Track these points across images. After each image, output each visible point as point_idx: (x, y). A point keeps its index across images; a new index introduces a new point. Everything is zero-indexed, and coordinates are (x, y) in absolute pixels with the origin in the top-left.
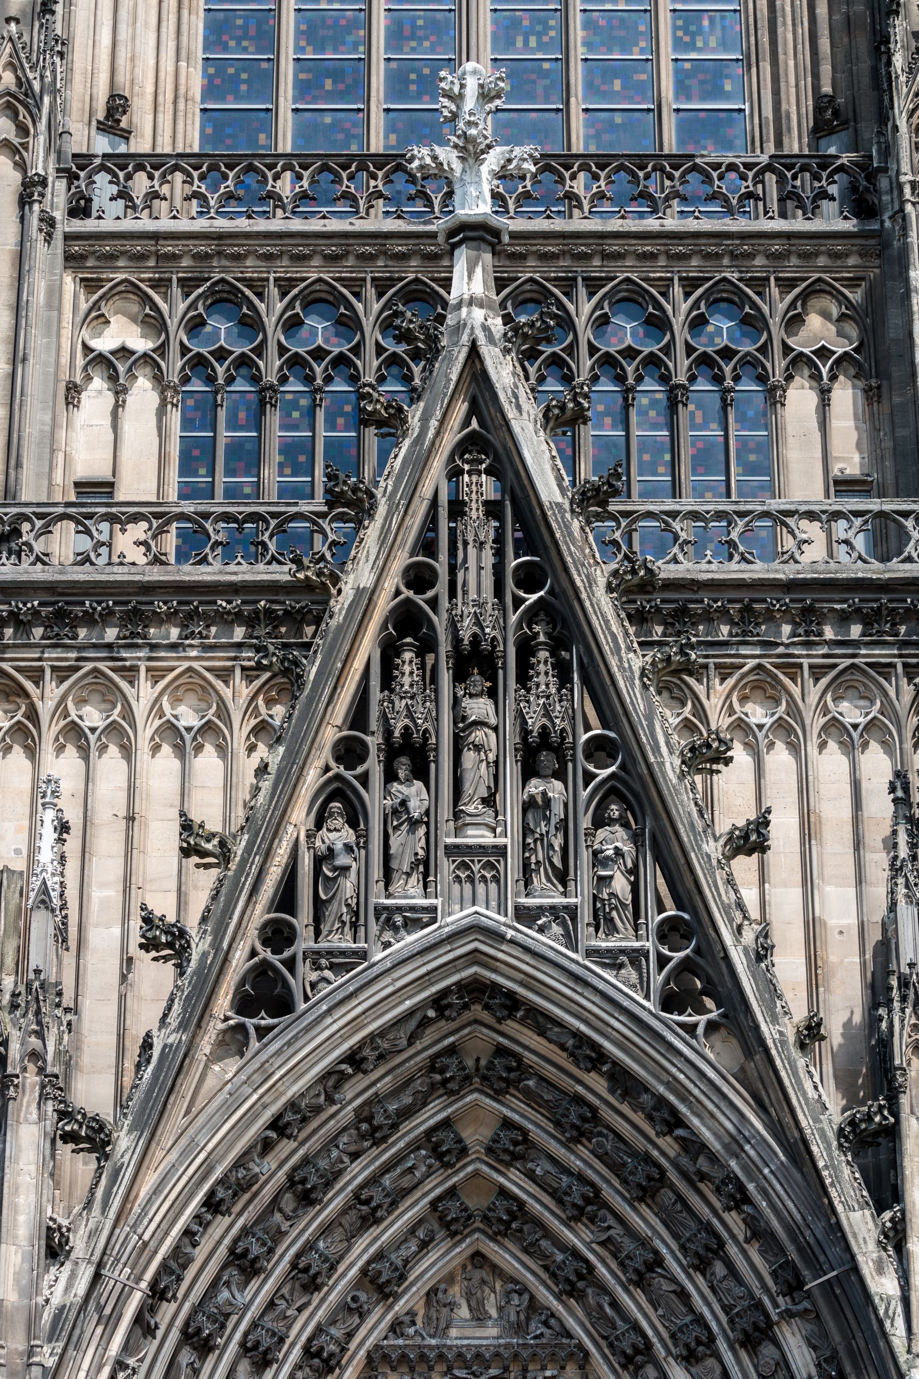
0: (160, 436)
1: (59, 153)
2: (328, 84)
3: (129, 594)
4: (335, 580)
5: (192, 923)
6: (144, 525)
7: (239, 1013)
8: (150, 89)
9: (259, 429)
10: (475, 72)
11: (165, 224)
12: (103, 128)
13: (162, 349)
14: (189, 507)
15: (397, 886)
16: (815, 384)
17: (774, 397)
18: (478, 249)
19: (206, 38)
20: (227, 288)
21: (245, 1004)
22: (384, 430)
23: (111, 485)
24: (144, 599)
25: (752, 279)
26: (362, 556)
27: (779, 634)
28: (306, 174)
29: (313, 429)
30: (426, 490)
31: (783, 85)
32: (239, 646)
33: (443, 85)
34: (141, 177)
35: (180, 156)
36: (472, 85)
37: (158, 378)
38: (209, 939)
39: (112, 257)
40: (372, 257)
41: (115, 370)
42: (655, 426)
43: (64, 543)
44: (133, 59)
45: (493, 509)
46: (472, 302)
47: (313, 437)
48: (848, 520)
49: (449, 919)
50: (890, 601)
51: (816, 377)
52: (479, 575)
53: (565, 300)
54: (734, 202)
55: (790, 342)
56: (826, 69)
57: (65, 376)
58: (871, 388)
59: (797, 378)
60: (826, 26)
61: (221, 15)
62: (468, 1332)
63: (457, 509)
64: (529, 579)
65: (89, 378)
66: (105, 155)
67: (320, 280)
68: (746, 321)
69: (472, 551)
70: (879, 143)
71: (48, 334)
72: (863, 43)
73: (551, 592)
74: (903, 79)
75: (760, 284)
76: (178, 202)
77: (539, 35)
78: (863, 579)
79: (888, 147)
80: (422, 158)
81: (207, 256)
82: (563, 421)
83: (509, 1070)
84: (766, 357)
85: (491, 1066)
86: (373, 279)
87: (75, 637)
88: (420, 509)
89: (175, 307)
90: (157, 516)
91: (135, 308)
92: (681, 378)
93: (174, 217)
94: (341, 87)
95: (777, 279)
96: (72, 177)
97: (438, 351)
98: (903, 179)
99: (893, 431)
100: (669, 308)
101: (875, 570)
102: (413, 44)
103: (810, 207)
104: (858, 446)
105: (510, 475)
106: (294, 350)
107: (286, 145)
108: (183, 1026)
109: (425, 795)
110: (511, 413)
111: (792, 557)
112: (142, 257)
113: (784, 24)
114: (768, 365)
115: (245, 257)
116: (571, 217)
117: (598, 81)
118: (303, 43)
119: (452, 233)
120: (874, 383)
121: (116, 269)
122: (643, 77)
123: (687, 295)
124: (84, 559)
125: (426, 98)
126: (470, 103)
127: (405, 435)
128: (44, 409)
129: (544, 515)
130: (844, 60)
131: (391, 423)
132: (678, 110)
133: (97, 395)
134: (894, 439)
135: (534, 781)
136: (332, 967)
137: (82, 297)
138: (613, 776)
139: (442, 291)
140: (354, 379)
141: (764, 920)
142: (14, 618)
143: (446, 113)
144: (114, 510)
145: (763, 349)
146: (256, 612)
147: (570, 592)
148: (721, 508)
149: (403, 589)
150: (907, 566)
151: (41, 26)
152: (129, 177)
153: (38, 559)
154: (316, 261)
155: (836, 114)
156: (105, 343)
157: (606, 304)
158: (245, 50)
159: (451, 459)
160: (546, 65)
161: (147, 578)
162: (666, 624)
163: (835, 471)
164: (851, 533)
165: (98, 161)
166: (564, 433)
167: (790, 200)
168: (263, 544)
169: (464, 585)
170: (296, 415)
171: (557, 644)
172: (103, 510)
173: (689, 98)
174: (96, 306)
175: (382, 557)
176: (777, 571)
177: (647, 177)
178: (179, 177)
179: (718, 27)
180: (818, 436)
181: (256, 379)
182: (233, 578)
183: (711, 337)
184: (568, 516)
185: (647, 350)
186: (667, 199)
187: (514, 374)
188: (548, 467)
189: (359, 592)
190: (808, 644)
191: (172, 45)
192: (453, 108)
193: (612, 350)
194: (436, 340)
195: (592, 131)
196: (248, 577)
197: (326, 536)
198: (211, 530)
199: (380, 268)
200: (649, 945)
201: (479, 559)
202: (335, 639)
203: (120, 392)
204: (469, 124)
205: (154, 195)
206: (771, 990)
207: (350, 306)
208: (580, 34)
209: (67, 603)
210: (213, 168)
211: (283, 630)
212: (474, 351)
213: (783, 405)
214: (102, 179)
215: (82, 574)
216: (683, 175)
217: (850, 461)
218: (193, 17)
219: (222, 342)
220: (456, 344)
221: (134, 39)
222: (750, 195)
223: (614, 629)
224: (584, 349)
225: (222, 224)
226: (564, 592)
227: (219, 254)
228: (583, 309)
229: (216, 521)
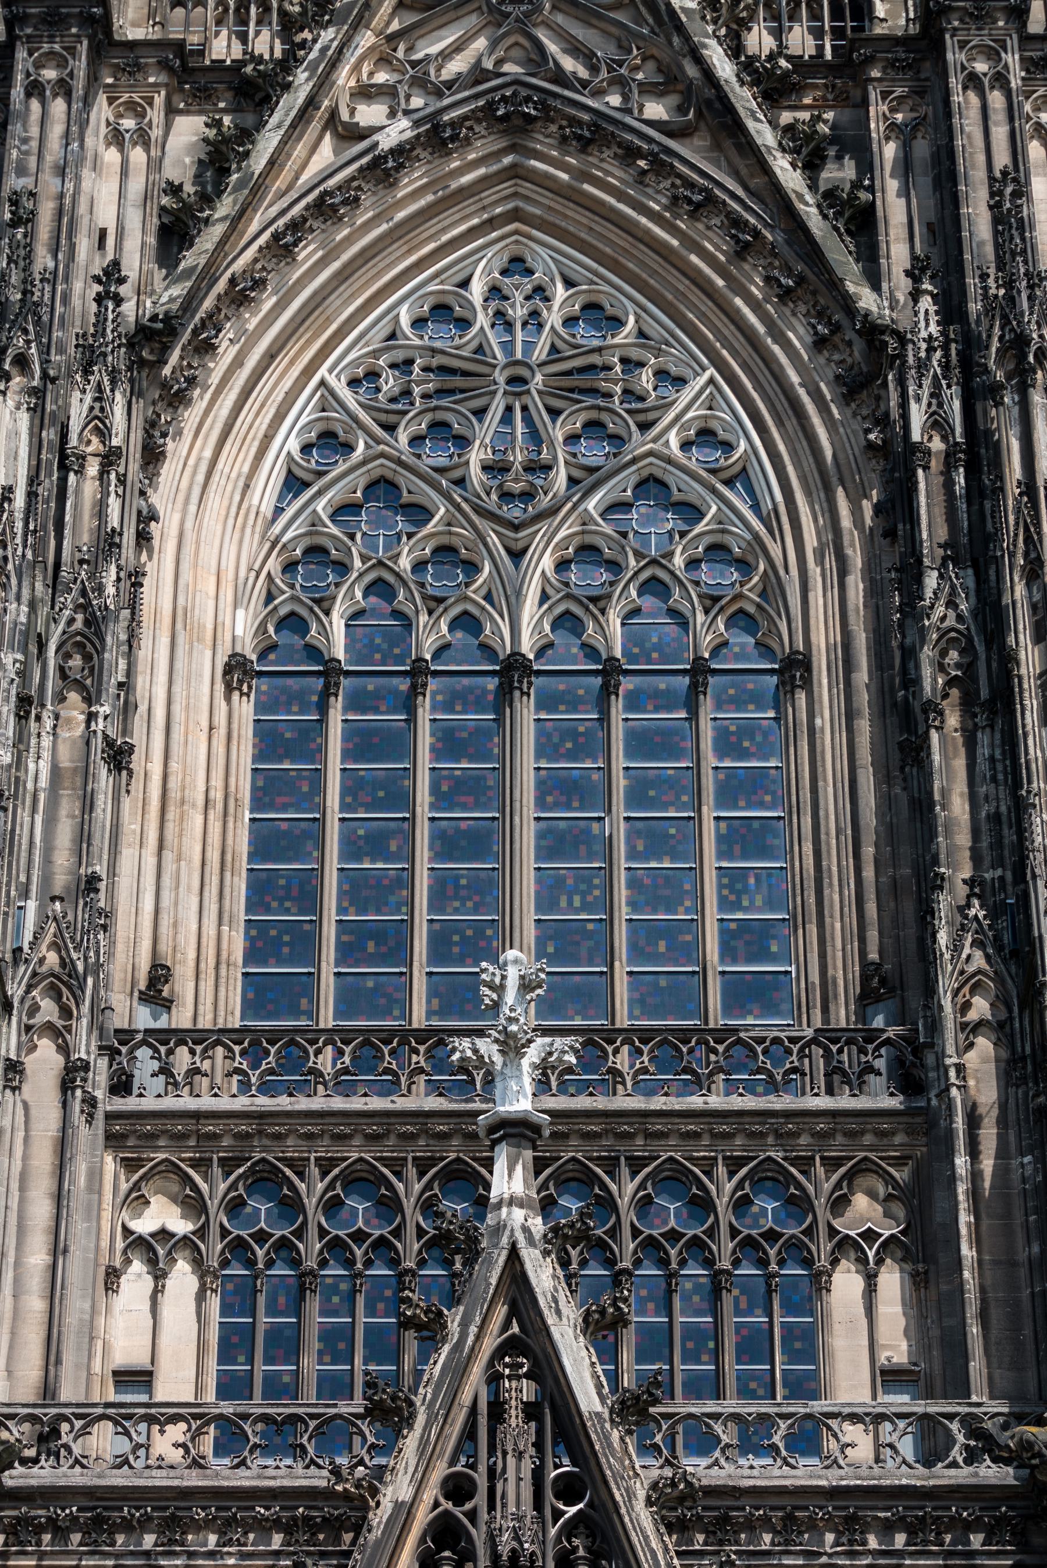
0: (199, 1322)
1: (101, 1029)
2: (371, 946)
3: (167, 1499)
4: (374, 1492)
6: (183, 1426)
8: (192, 955)
9: (298, 1316)
10: (516, 961)
11: (206, 1103)
12: (145, 998)
13: (202, 1232)
14: (227, 1408)
16: (861, 1267)
17: (819, 1282)
18: (518, 1146)
19: (248, 899)
20: (267, 1168)
22: (425, 1333)
23: (150, 1374)
24: (183, 1504)
25: (797, 1158)
26: (401, 1467)
27: (822, 1543)
28: (347, 1050)
29: (353, 1315)
30: (466, 1397)
31: (829, 949)
32: (277, 1554)
33: (484, 976)
34: (183, 1052)
35: (221, 1031)
36: (513, 974)
37: (198, 1262)
39: (152, 1136)
40: (413, 1137)
41: (155, 1253)
42: (698, 1313)
43: (104, 1441)
44: (175, 925)
45: (531, 1411)
46: (512, 1201)
47: (353, 1323)
48: (893, 1422)
50: (934, 1509)
51: (862, 1260)
52: (518, 1486)
53: (607, 1179)
54: (779, 1078)
55: (837, 1224)
56: (873, 935)
57: (105, 1261)
58: (918, 1274)
59: (843, 1262)
60: (873, 890)
61: (264, 874)
63: (497, 1411)
64: (568, 1489)
65: (128, 1262)
66: (146, 1031)
67: (361, 1160)
68: (791, 1200)
69: (511, 1461)
70: (925, 1017)
71: (88, 1219)
72: (909, 908)
73: (590, 1505)
74: (947, 956)
75: (805, 1164)
76: (218, 1080)
77: (584, 895)
78: (907, 1486)
79: (934, 1021)
80: (463, 1051)
81: (248, 1136)
82: (602, 1328)
84: (811, 1240)
86: (414, 1159)
87: (113, 1544)
88: (460, 1417)
89: (216, 1188)
90: (196, 1417)
91: (175, 1188)
92: (725, 1264)
93: (216, 1095)
94: (384, 949)
95: (822, 1158)
96: (112, 1053)
97: (478, 1253)
98: (948, 1061)
99: (940, 1319)
100: (712, 1188)
101: (917, 1477)
102: (457, 904)
103: (855, 1083)
104: (906, 1333)
105: (550, 1381)
106: (335, 1232)
107: (327, 1019)
110: (551, 1319)
111: (835, 1461)
112: (183, 1136)
113: (831, 885)
114: (814, 1248)
115: (287, 1136)
116: (615, 1094)
117: (642, 942)
118: (345, 904)
119: (492, 1129)
120: (921, 1267)
121: (157, 1149)
122: (689, 938)
123: (731, 1174)
124: (123, 1462)
125: (469, 961)
126: (510, 997)
127: (444, 1340)
128: (83, 1297)
129: (584, 1425)
130: (890, 926)
131: (431, 1331)
132: (723, 973)
133: (137, 1278)
134: (942, 1328)
137: (123, 1177)
139: (483, 1171)
140: (394, 1262)
142: (54, 1526)
143: (487, 1001)
144: (153, 1411)
145: (809, 1232)
146: (294, 1518)
147: (610, 1505)
148: (763, 1410)
149: (442, 1500)
150: (953, 1472)
151: (86, 904)
152: (170, 1052)
153: (77, 1461)
154: (356, 1142)
155: (883, 982)
156: (145, 1225)
157: (649, 1184)
158: (287, 911)
159: (491, 1364)
160: (590, 926)
161: (185, 1484)
162: (708, 1533)
163: (882, 1359)
164: (895, 1436)
165: (139, 1037)
166: (604, 1337)
167: (836, 1078)
168: (302, 1447)
169: (503, 1497)
170: (336, 1299)
172: (142, 1411)
173: (735, 961)
174: (136, 1187)
175: (421, 1469)
176: (820, 1477)
177: (691, 1051)
178: (220, 1051)
179: (765, 885)
180: (864, 1322)
181: (295, 1262)
182: (271, 1483)
183: (756, 1218)
184: (608, 1425)
185: (690, 1233)
186: (711, 1074)
187: (555, 1276)
188: (587, 1374)
189: (398, 1505)
190: (851, 1554)
191: (214, 908)
192: (495, 996)
193: (655, 1233)
194: (476, 1241)
195: (636, 995)
196: (287, 1483)
197: (364, 1439)
198: (250, 1432)
199: (421, 1148)
201: (518, 1470)
202: (373, 1555)
203: (159, 1276)
204: (511, 1020)
205: (194, 1071)
207: (390, 1187)
208: (624, 892)
209: (105, 1508)
210: (253, 1043)
211: (321, 1537)
212: (514, 1252)
213: (829, 1291)
214: (143, 1053)
215: (119, 1479)
216: (727, 1049)
217: (897, 1350)
218: (236, 879)
219: (263, 1224)
220: (496, 1245)
221: (176, 904)
222: (794, 1070)
223: (654, 1545)
224: (627, 1232)
225: (264, 1102)
226: (604, 1505)
227: (260, 1132)
228: (626, 1190)
229: (255, 1422)
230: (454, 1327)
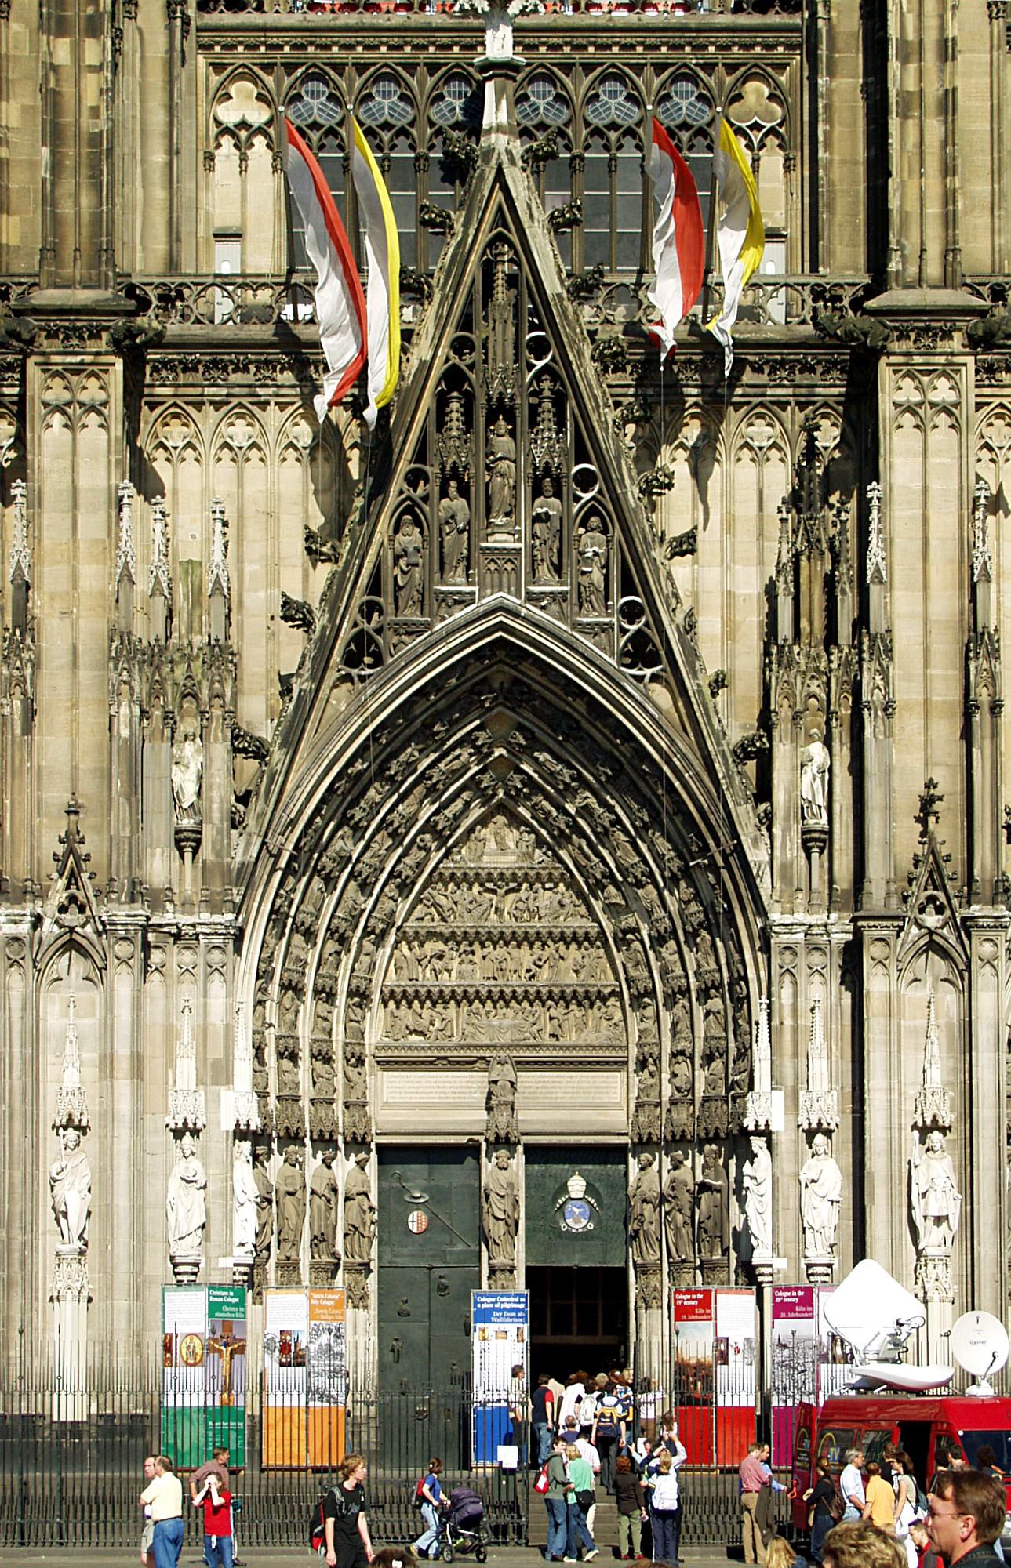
5: (315, 604)
6: (269, 291)
7: (346, 664)
15: (448, 576)
21: (352, 659)
38: (327, 615)
46: (499, 129)
49: (483, 601)
62: (496, 858)
65: (219, 146)
83: (522, 693)
85: (510, 691)
108: (312, 677)
109: (467, 510)
135: (539, 501)
136: (409, 634)
138: (593, 498)
141: (695, 595)
171: (559, 401)
187: (529, 188)
189: (422, 363)
200: (614, 620)
206: (692, 655)
227: (311, 43)
230: (458, 228)
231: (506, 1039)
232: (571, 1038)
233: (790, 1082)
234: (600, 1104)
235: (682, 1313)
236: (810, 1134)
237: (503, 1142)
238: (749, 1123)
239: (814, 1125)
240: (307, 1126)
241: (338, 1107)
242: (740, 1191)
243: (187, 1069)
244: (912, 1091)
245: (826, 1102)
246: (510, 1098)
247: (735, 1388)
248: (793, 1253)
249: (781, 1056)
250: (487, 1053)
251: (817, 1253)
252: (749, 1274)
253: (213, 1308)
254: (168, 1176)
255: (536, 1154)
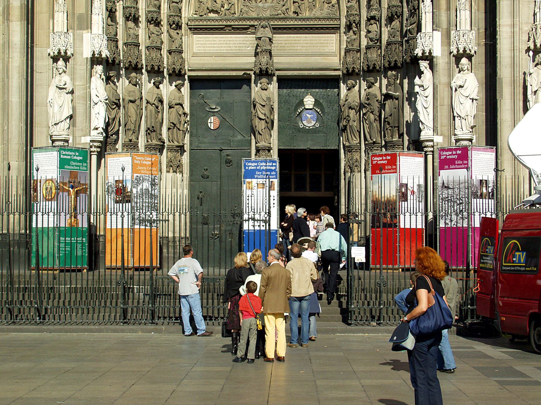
231: (267, 14)
232: (307, 14)
233: (444, 25)
234: (324, 52)
235: (377, 169)
236: (458, 58)
237: (264, 74)
238: (418, 52)
239: (461, 51)
240: (144, 62)
241: (164, 53)
242: (412, 96)
243: (60, 19)
244: (526, 28)
245: (470, 38)
246: (269, 48)
247: (411, 219)
248: (446, 133)
249: (439, 9)
250: (256, 23)
251: (463, 131)
252: (417, 146)
253: (63, 163)
254: (49, 86)
255: (285, 82)
